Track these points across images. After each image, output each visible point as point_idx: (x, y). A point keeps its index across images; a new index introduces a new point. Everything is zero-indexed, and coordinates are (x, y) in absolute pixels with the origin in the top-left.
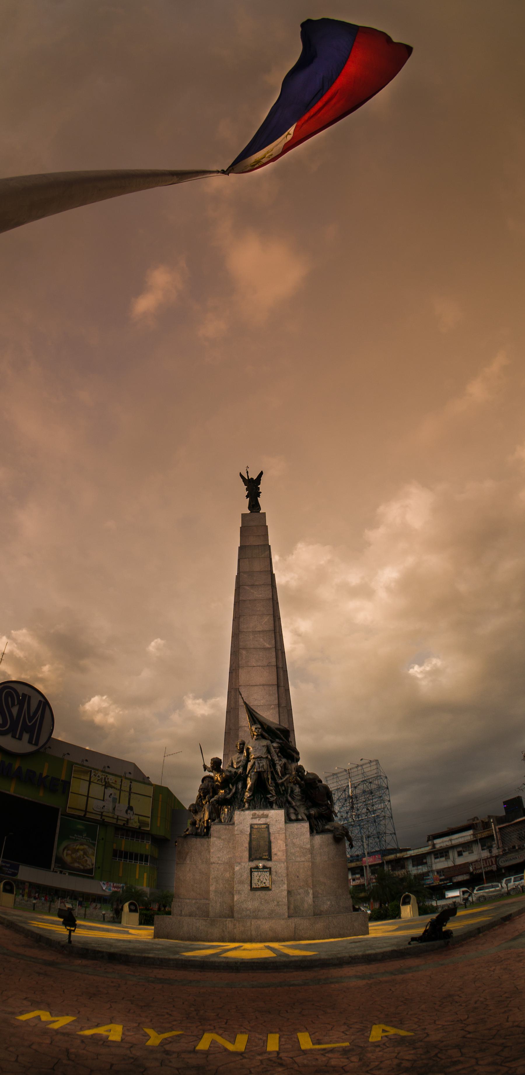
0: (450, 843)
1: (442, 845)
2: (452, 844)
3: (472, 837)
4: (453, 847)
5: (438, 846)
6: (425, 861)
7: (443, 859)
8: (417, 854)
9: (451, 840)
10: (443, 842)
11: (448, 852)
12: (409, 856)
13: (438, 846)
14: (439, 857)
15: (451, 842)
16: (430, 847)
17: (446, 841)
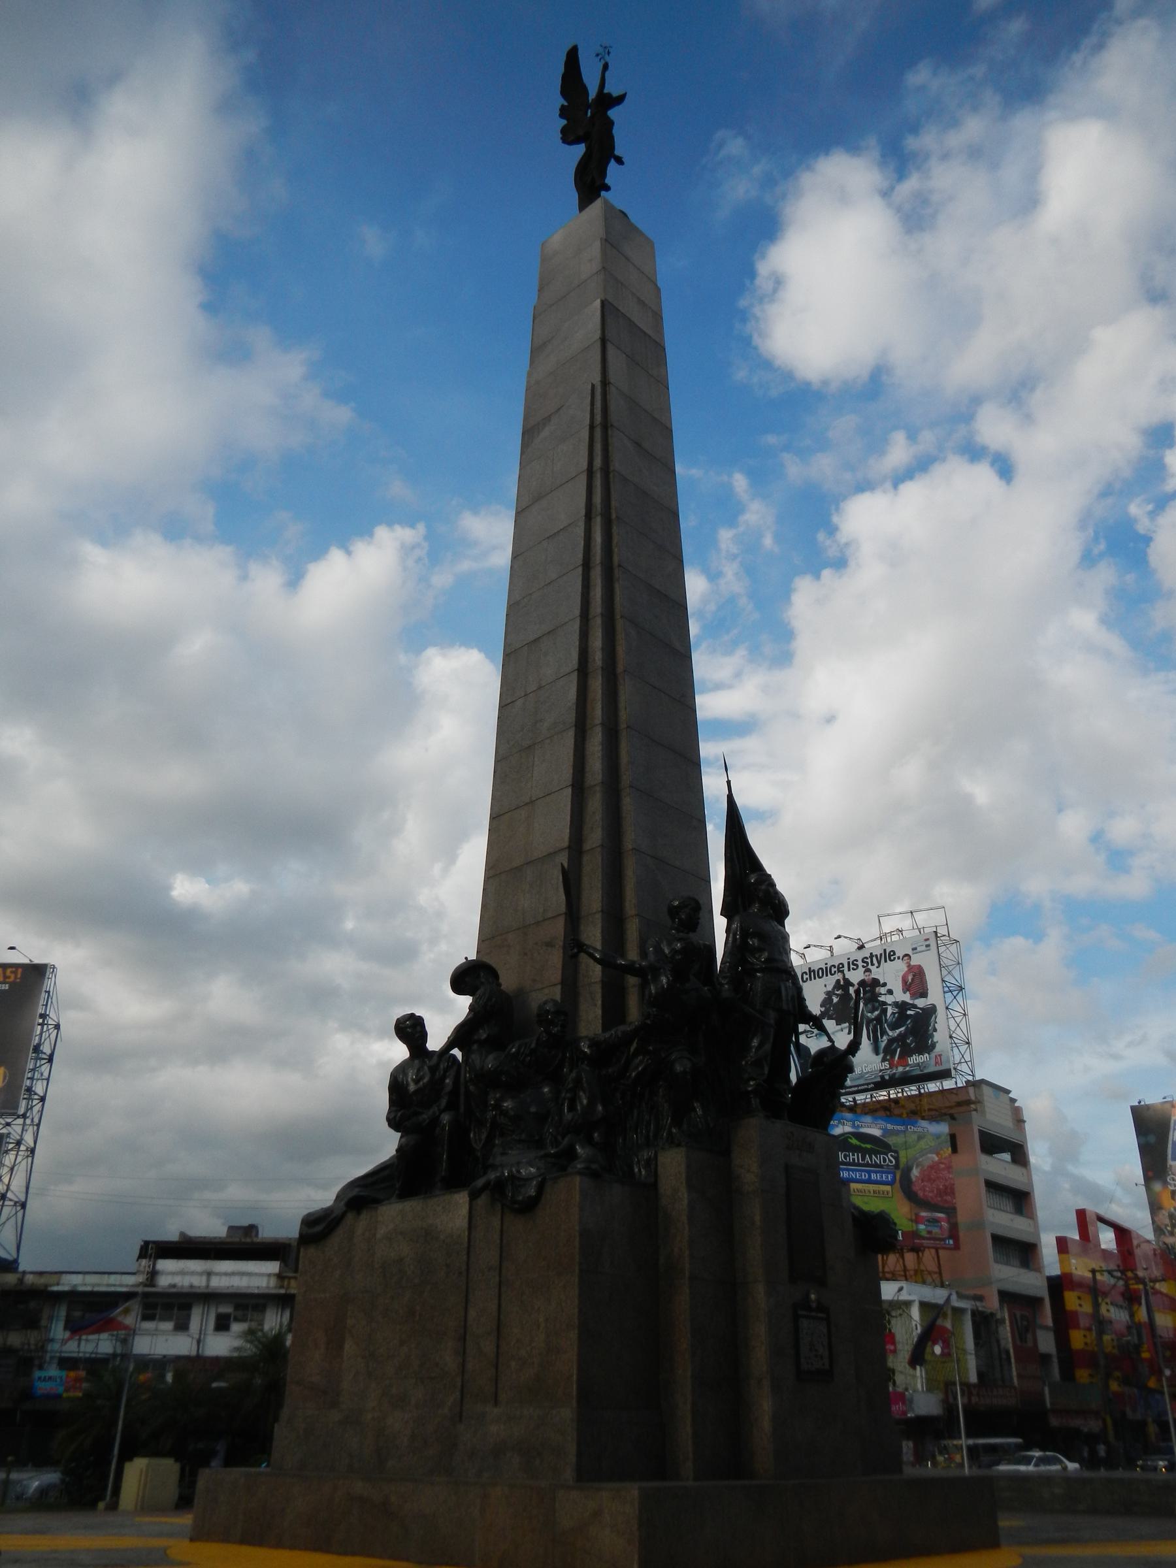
0: (204, 1283)
1: (177, 1280)
2: (208, 1286)
3: (273, 1282)
4: (208, 1298)
5: (163, 1282)
7: (168, 1326)
8: (96, 1289)
9: (209, 1274)
10: (182, 1273)
12: (66, 1288)
13: (163, 1282)
14: (157, 1317)
15: (208, 1280)
16: (141, 1278)
17: (193, 1273)
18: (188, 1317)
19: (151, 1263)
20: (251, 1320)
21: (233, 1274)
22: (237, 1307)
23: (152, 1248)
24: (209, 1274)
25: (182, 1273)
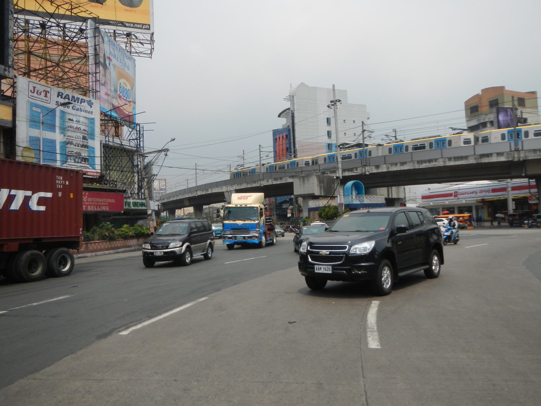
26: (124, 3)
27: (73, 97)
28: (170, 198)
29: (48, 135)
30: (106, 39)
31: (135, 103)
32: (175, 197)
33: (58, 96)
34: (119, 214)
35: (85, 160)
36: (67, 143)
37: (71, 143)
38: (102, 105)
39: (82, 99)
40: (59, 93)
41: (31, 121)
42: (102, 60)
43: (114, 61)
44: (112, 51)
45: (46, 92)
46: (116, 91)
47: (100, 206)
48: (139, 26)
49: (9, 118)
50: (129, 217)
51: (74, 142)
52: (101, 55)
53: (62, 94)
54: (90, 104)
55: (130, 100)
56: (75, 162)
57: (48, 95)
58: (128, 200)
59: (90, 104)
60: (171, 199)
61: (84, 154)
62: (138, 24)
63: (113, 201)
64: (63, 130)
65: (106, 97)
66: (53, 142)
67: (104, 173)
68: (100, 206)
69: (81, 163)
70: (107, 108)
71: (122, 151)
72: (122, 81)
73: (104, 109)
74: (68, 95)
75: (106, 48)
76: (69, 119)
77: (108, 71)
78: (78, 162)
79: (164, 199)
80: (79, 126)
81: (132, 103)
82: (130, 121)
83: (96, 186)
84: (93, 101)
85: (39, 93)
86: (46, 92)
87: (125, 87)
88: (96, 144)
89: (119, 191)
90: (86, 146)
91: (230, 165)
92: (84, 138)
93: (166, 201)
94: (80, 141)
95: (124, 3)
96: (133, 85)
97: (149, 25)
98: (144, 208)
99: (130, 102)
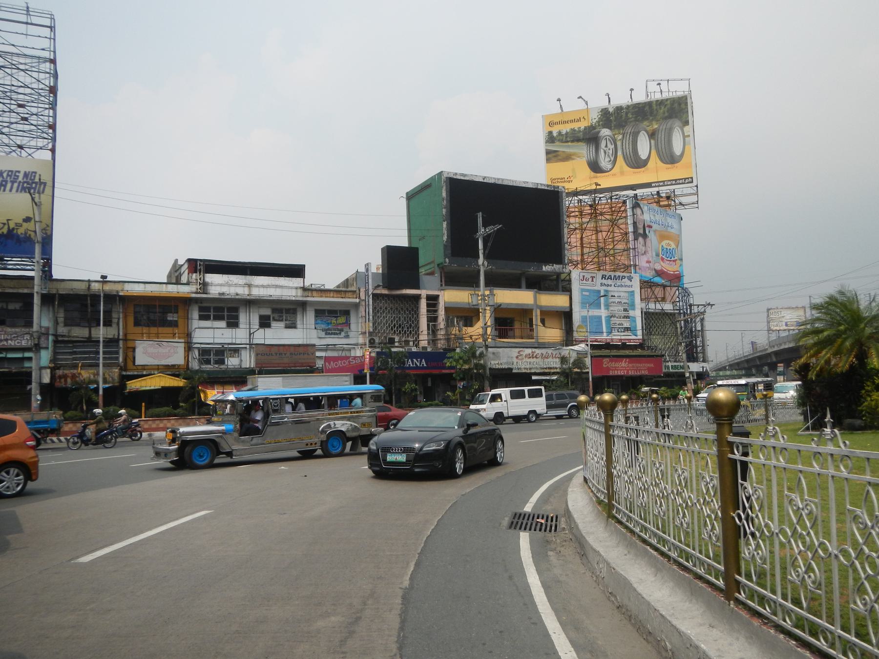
0: (247, 292)
1: (225, 290)
4: (250, 303)
6: (170, 317)
7: (223, 324)
10: (228, 285)
11: (236, 310)
13: (214, 291)
16: (193, 288)
17: (236, 285)
18: (237, 317)
19: (202, 276)
20: (286, 320)
21: (268, 286)
22: (274, 311)
23: (200, 265)
24: (250, 286)
25: (228, 285)
26: (665, 161)
27: (615, 276)
28: (781, 344)
29: (594, 312)
30: (645, 208)
31: (681, 260)
32: (787, 343)
33: (602, 279)
34: (661, 377)
35: (627, 329)
36: (611, 317)
37: (614, 316)
38: (644, 274)
39: (622, 276)
40: (603, 275)
41: (582, 303)
42: (641, 231)
43: (655, 227)
44: (652, 218)
45: (593, 277)
46: (657, 255)
47: (639, 370)
48: (681, 181)
49: (568, 305)
50: (674, 379)
51: (617, 316)
52: (640, 226)
53: (606, 276)
54: (630, 279)
55: (676, 258)
56: (618, 332)
57: (594, 279)
58: (667, 364)
59: (630, 279)
60: (782, 347)
61: (626, 324)
62: (680, 179)
63: (652, 365)
64: (607, 306)
65: (648, 265)
66: (600, 317)
67: (646, 338)
68: (639, 370)
69: (624, 332)
70: (649, 275)
71: (663, 314)
72: (664, 243)
73: (645, 277)
74: (610, 276)
75: (647, 215)
76: (612, 296)
77: (648, 240)
78: (621, 332)
79: (774, 346)
80: (619, 300)
81: (678, 261)
82: (676, 279)
83: (639, 352)
84: (633, 275)
85: (587, 280)
86: (593, 277)
87: (669, 248)
88: (637, 314)
89: (657, 356)
90: (627, 317)
91: (869, 294)
92: (625, 310)
93: (776, 349)
94: (623, 314)
95: (665, 161)
96: (678, 243)
97: (692, 178)
98: (683, 371)
99: (674, 261)
